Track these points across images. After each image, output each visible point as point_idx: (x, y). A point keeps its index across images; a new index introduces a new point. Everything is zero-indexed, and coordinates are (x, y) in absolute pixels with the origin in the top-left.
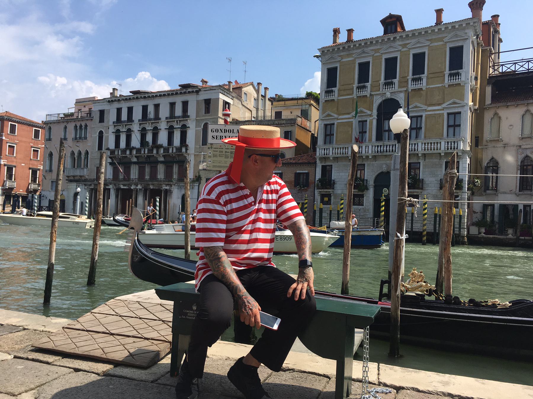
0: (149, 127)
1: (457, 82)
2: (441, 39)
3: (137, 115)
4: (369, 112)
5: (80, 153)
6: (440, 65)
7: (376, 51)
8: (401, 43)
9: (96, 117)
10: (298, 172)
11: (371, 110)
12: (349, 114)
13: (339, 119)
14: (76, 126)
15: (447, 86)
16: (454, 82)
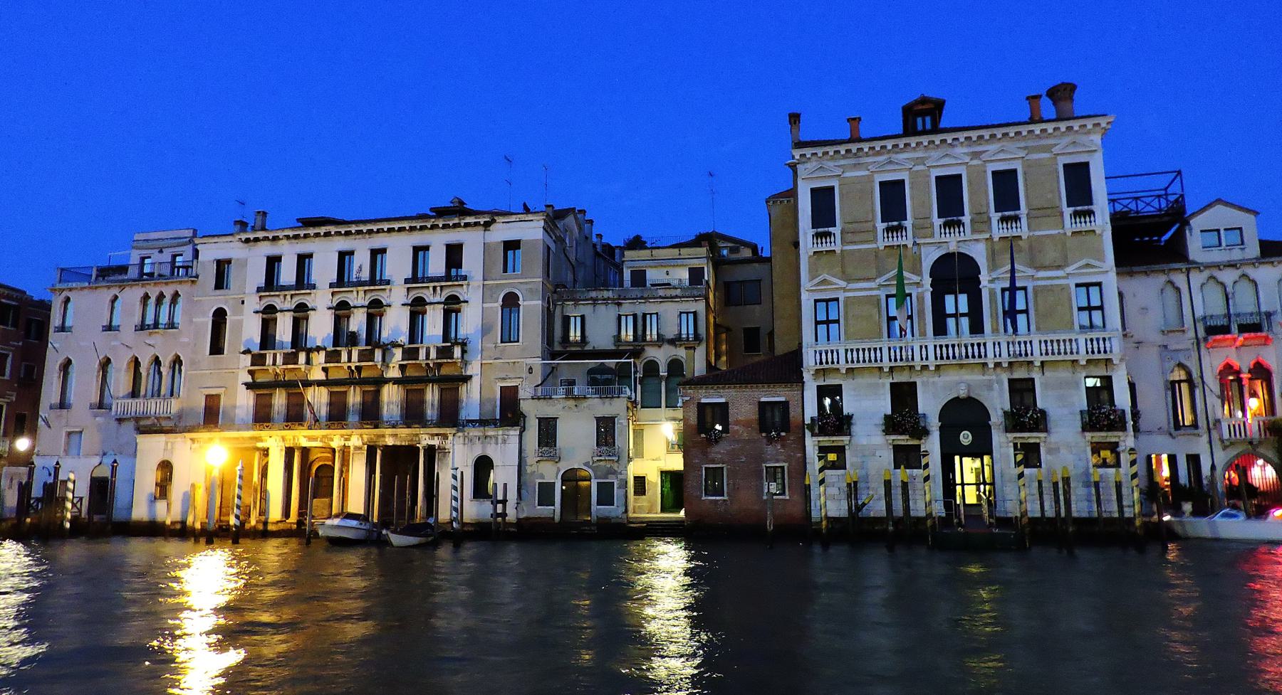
0: (358, 298)
1: (1088, 227)
2: (1048, 149)
3: (324, 270)
4: (916, 279)
5: (157, 361)
6: (1049, 196)
7: (921, 161)
8: (965, 150)
9: (208, 275)
10: (763, 399)
11: (919, 273)
12: (868, 279)
13: (850, 290)
14: (146, 297)
15: (1069, 234)
16: (1084, 227)
